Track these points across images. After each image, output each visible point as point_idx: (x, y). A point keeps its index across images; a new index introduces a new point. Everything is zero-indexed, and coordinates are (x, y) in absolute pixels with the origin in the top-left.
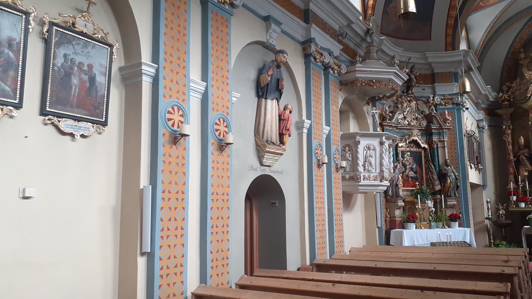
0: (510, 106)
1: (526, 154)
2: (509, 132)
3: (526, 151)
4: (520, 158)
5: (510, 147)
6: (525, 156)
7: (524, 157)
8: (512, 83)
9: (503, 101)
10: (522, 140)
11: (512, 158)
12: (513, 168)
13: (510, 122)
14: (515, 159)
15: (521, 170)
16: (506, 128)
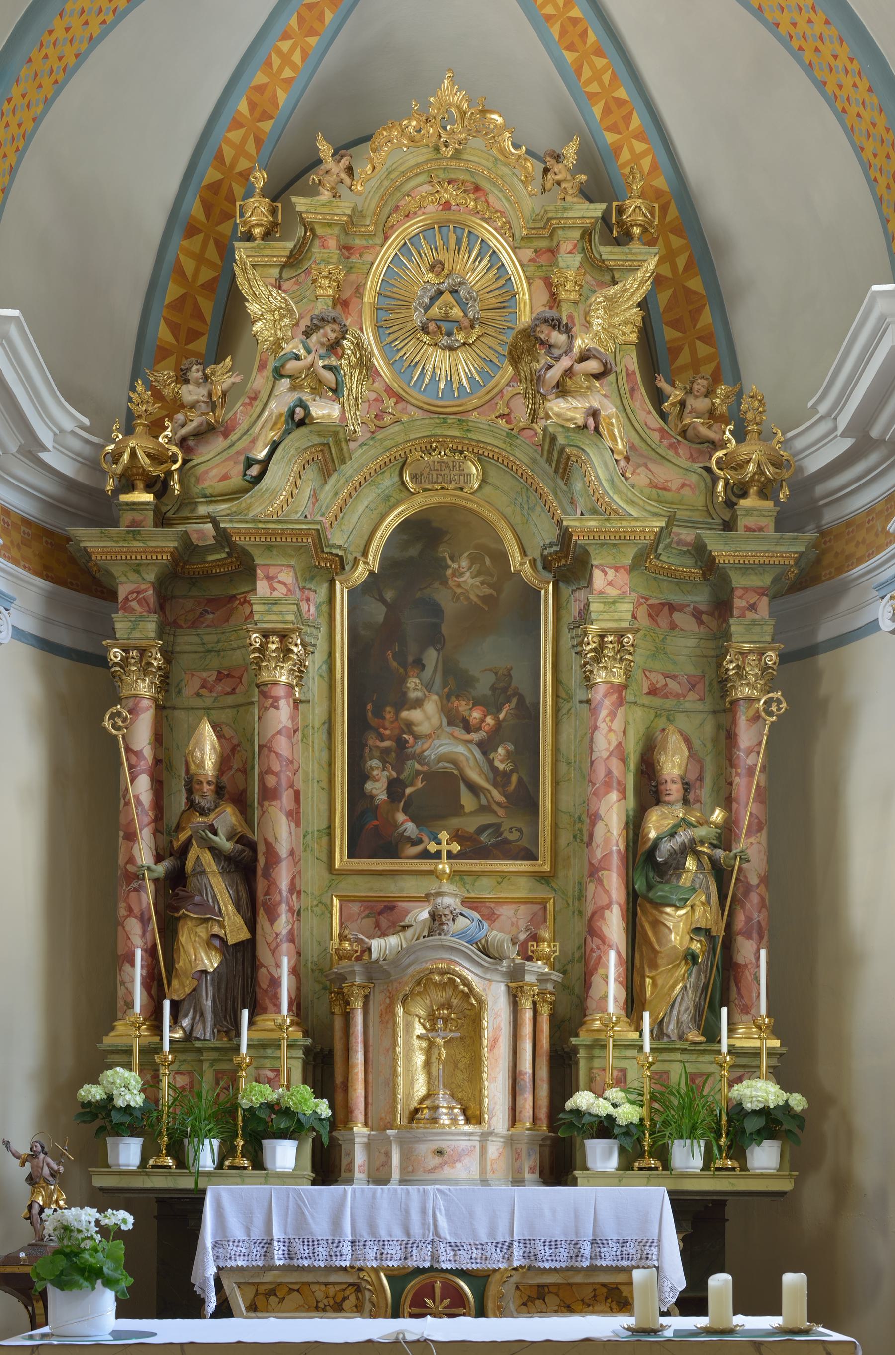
0: (162, 520)
1: (222, 841)
2: (144, 688)
3: (227, 817)
4: (190, 864)
5: (141, 789)
6: (215, 851)
7: (207, 858)
8: (183, 378)
9: (127, 484)
10: (207, 750)
11: (144, 852)
12: (144, 920)
13: (150, 626)
14: (161, 869)
15: (184, 937)
16: (125, 662)
